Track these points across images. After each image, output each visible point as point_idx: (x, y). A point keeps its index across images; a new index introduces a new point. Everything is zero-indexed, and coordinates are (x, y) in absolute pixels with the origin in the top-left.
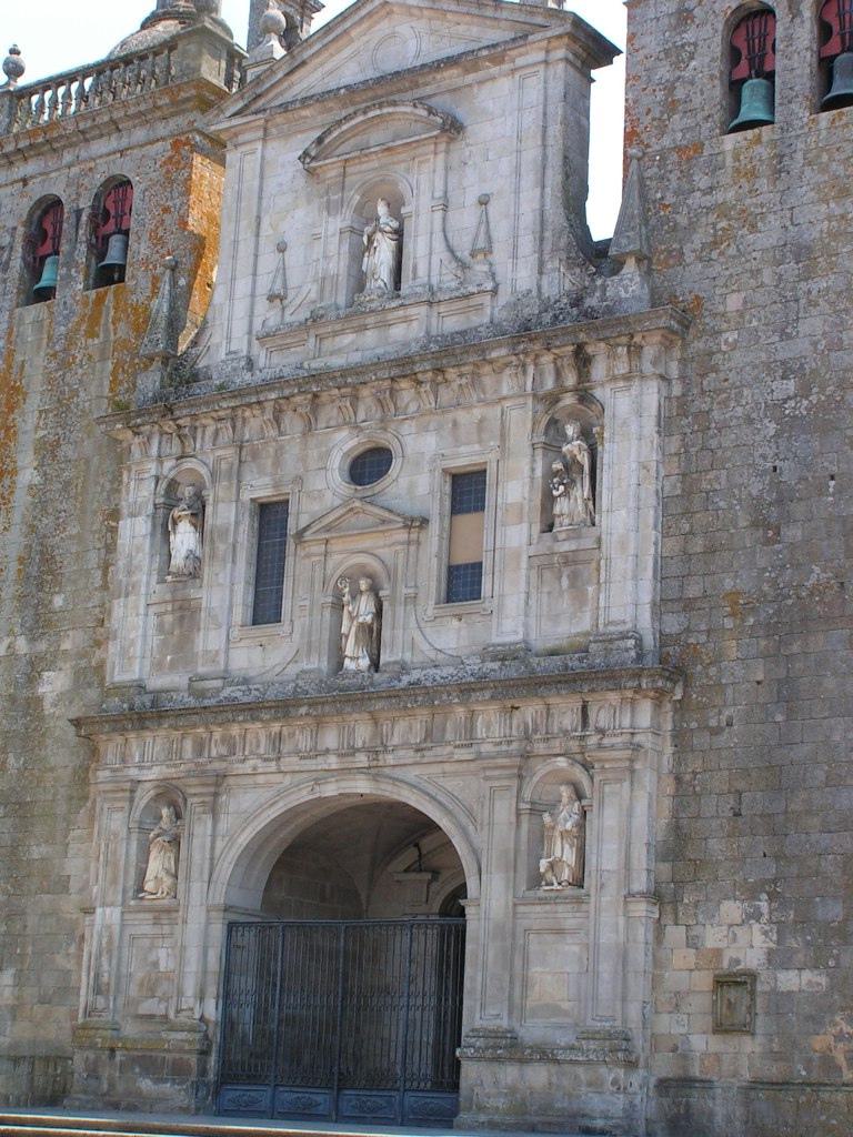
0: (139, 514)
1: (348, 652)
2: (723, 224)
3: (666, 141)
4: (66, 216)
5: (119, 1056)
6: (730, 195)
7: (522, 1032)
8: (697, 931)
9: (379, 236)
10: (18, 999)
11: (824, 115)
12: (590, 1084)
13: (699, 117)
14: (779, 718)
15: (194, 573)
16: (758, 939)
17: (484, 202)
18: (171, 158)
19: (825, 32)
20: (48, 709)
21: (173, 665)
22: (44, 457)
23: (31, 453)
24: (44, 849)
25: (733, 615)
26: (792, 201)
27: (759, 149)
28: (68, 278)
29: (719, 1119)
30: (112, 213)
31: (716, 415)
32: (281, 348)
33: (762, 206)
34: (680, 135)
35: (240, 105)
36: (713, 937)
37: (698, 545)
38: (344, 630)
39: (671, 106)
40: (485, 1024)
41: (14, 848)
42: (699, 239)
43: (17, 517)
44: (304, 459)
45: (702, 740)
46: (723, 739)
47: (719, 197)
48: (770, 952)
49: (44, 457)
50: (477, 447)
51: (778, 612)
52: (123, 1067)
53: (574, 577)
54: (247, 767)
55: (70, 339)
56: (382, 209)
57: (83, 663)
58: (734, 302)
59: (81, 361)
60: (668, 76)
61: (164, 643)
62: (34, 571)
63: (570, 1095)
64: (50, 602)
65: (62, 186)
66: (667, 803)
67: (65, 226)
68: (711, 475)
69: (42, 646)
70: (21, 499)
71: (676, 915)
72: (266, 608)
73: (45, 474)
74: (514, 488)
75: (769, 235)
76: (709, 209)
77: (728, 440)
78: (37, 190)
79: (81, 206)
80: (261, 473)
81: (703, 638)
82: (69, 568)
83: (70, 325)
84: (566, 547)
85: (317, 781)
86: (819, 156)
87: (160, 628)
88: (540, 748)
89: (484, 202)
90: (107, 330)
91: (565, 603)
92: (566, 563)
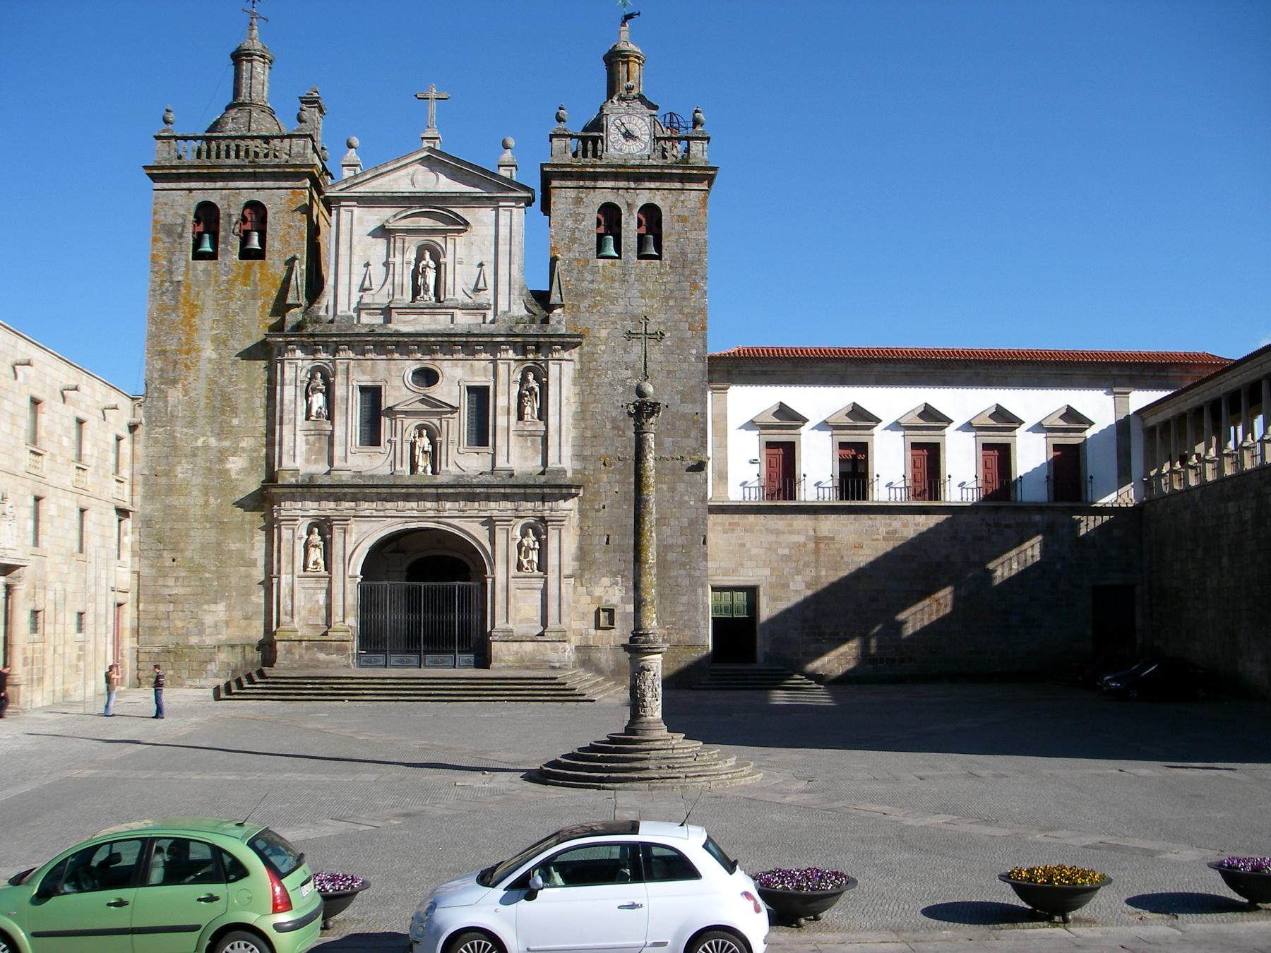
0: (290, 384)
1: (419, 464)
2: (599, 298)
3: (571, 255)
4: (221, 216)
5: (304, 643)
6: (602, 286)
7: (515, 630)
8: (590, 589)
9: (428, 269)
10: (229, 617)
11: (643, 261)
12: (552, 649)
13: (587, 248)
14: (625, 507)
15: (330, 417)
16: (617, 592)
17: (481, 265)
18: (291, 199)
19: (640, 224)
20: (234, 476)
21: (316, 461)
22: (218, 345)
23: (209, 342)
24: (238, 545)
25: (604, 464)
26: (629, 295)
27: (613, 269)
28: (227, 251)
29: (602, 660)
30: (249, 219)
31: (596, 380)
32: (370, 314)
33: (616, 294)
34: (578, 254)
35: (345, 186)
36: (598, 591)
37: (588, 433)
38: (417, 453)
39: (573, 240)
40: (500, 627)
41: (219, 544)
42: (586, 303)
43: (202, 375)
44: (389, 371)
45: (592, 514)
46: (602, 513)
47: (595, 286)
48: (622, 597)
49: (218, 345)
50: (484, 379)
51: (624, 465)
52: (307, 647)
53: (533, 442)
54: (367, 513)
55: (231, 283)
56: (427, 255)
57: (255, 455)
58: (604, 333)
59: (240, 297)
60: (571, 226)
61: (309, 451)
62: (218, 404)
63: (543, 654)
64: (231, 422)
65: (218, 198)
66: (577, 538)
67: (221, 221)
68: (594, 405)
69: (227, 444)
70: (205, 368)
71: (582, 581)
72: (372, 437)
73: (220, 354)
74: (504, 400)
75: (619, 308)
76: (592, 291)
77: (602, 390)
78: (199, 197)
79: (232, 212)
80: (364, 372)
81: (592, 473)
82: (242, 405)
83: (230, 277)
84: (530, 428)
85: (406, 522)
86: (640, 278)
87: (307, 443)
88: (522, 514)
89: (481, 265)
90: (256, 285)
91: (530, 452)
92: (530, 436)
